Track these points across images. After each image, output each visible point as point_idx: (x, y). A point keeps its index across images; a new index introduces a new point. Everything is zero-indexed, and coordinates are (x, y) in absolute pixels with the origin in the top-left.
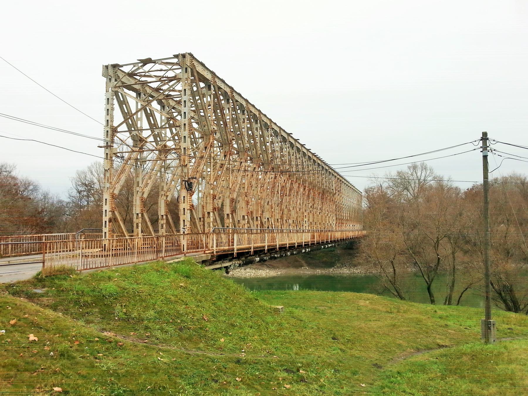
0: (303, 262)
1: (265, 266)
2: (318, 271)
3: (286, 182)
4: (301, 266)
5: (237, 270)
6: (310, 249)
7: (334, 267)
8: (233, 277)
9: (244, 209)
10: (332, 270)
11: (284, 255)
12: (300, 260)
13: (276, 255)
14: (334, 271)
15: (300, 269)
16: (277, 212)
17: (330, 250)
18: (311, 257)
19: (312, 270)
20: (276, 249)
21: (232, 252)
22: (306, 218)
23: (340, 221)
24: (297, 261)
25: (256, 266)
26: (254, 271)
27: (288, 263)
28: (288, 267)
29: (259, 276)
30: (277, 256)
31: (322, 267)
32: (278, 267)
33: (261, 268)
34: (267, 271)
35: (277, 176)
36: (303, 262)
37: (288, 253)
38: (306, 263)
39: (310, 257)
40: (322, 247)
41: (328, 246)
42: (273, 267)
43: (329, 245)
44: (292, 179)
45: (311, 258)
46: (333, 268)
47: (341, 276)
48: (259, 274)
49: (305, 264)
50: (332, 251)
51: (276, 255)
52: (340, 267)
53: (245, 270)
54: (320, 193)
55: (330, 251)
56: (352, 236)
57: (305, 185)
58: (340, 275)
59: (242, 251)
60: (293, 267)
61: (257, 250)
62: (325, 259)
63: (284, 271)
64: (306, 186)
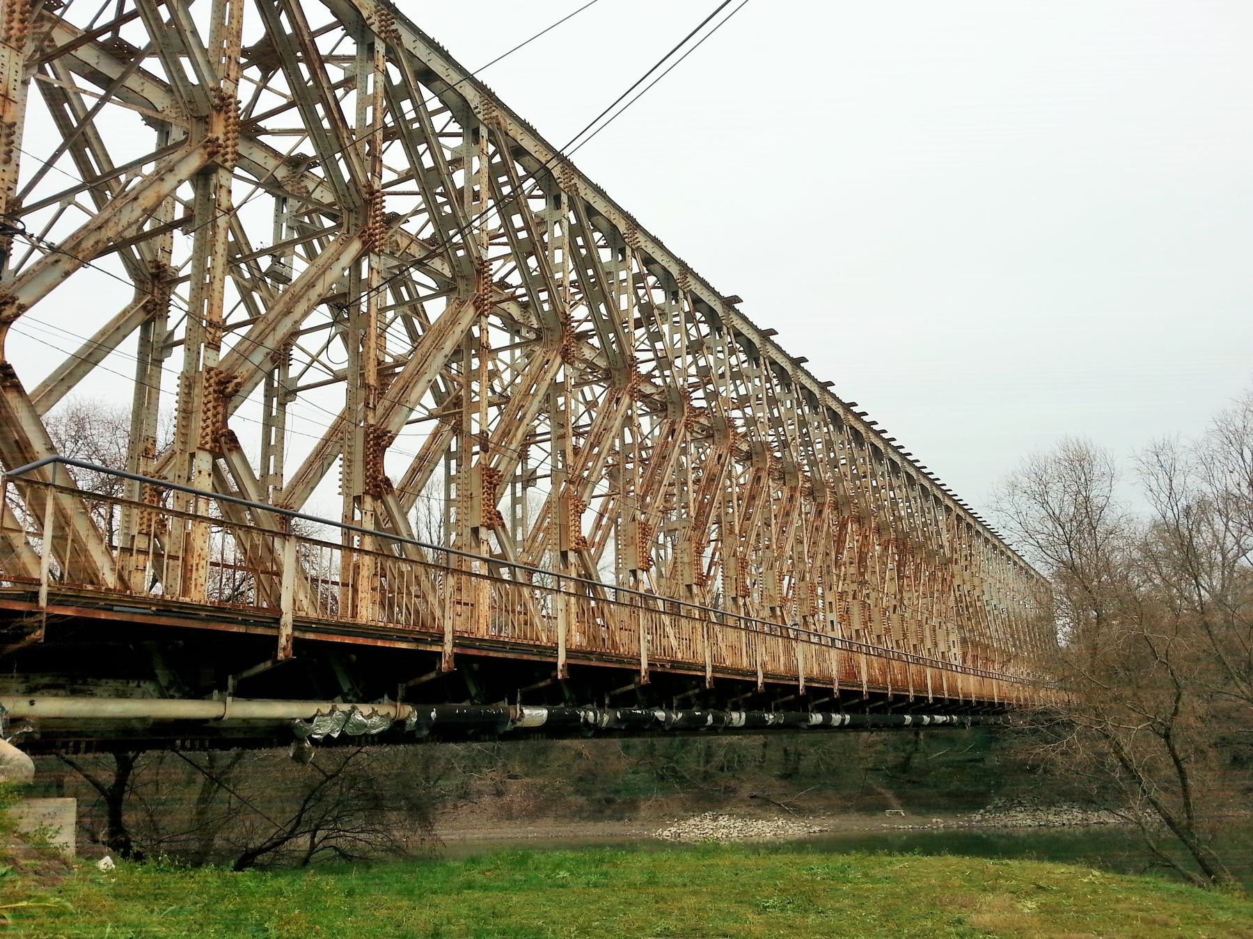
0: (889, 794)
1: (774, 808)
2: (934, 820)
3: (722, 460)
4: (882, 807)
5: (692, 821)
6: (848, 717)
7: (984, 808)
8: (680, 842)
9: (476, 502)
10: (979, 817)
11: (710, 718)
12: (879, 790)
13: (660, 714)
14: (987, 821)
15: (879, 816)
16: (686, 559)
17: (969, 757)
18: (914, 778)
19: (918, 819)
20: (637, 679)
21: (270, 632)
22: (831, 612)
23: (975, 647)
24: (868, 791)
25: (747, 809)
26: (739, 824)
27: (844, 798)
28: (845, 810)
29: (757, 838)
30: (668, 718)
31: (947, 809)
32: (812, 812)
33: (763, 814)
34: (780, 823)
35: (676, 427)
36: (888, 795)
37: (735, 715)
38: (899, 796)
39: (909, 781)
40: (908, 718)
41: (933, 719)
42: (795, 811)
43: (936, 717)
44: (760, 465)
45: (914, 782)
46: (982, 811)
47: (1009, 837)
48: (753, 834)
49: (894, 802)
50: (976, 761)
51: (660, 714)
52: (1006, 809)
53: (715, 820)
54: (889, 541)
55: (971, 761)
56: (1026, 699)
57: (819, 500)
58: (1005, 831)
59: (370, 642)
60: (858, 811)
61: (491, 654)
62: (955, 784)
63: (831, 822)
64: (823, 504)
